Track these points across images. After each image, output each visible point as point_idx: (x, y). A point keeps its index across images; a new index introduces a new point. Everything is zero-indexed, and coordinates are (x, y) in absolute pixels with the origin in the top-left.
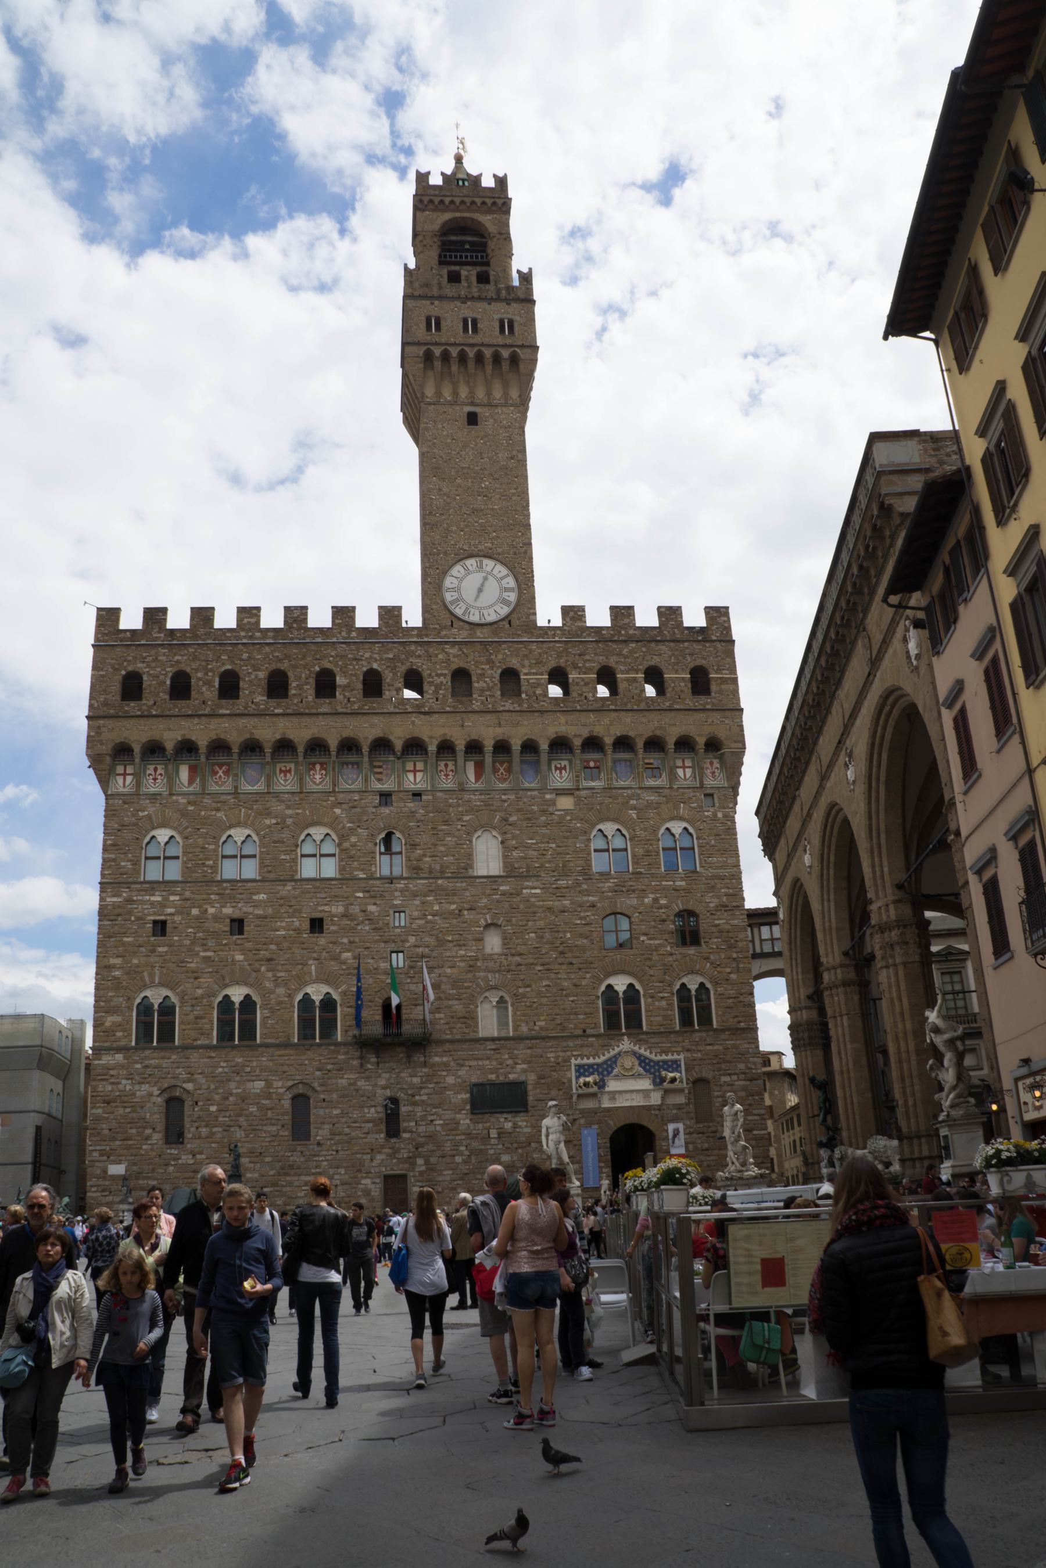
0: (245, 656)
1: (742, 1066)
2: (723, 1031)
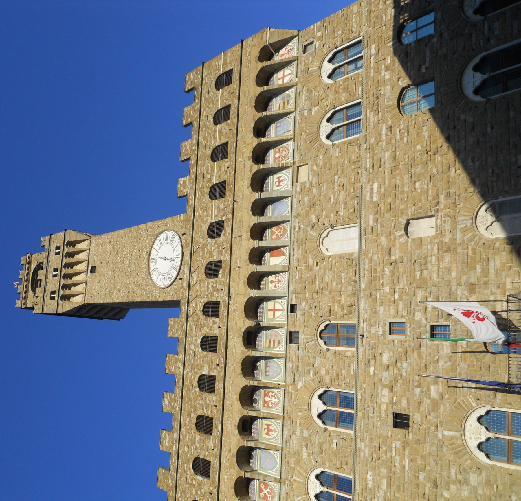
0: (186, 449)
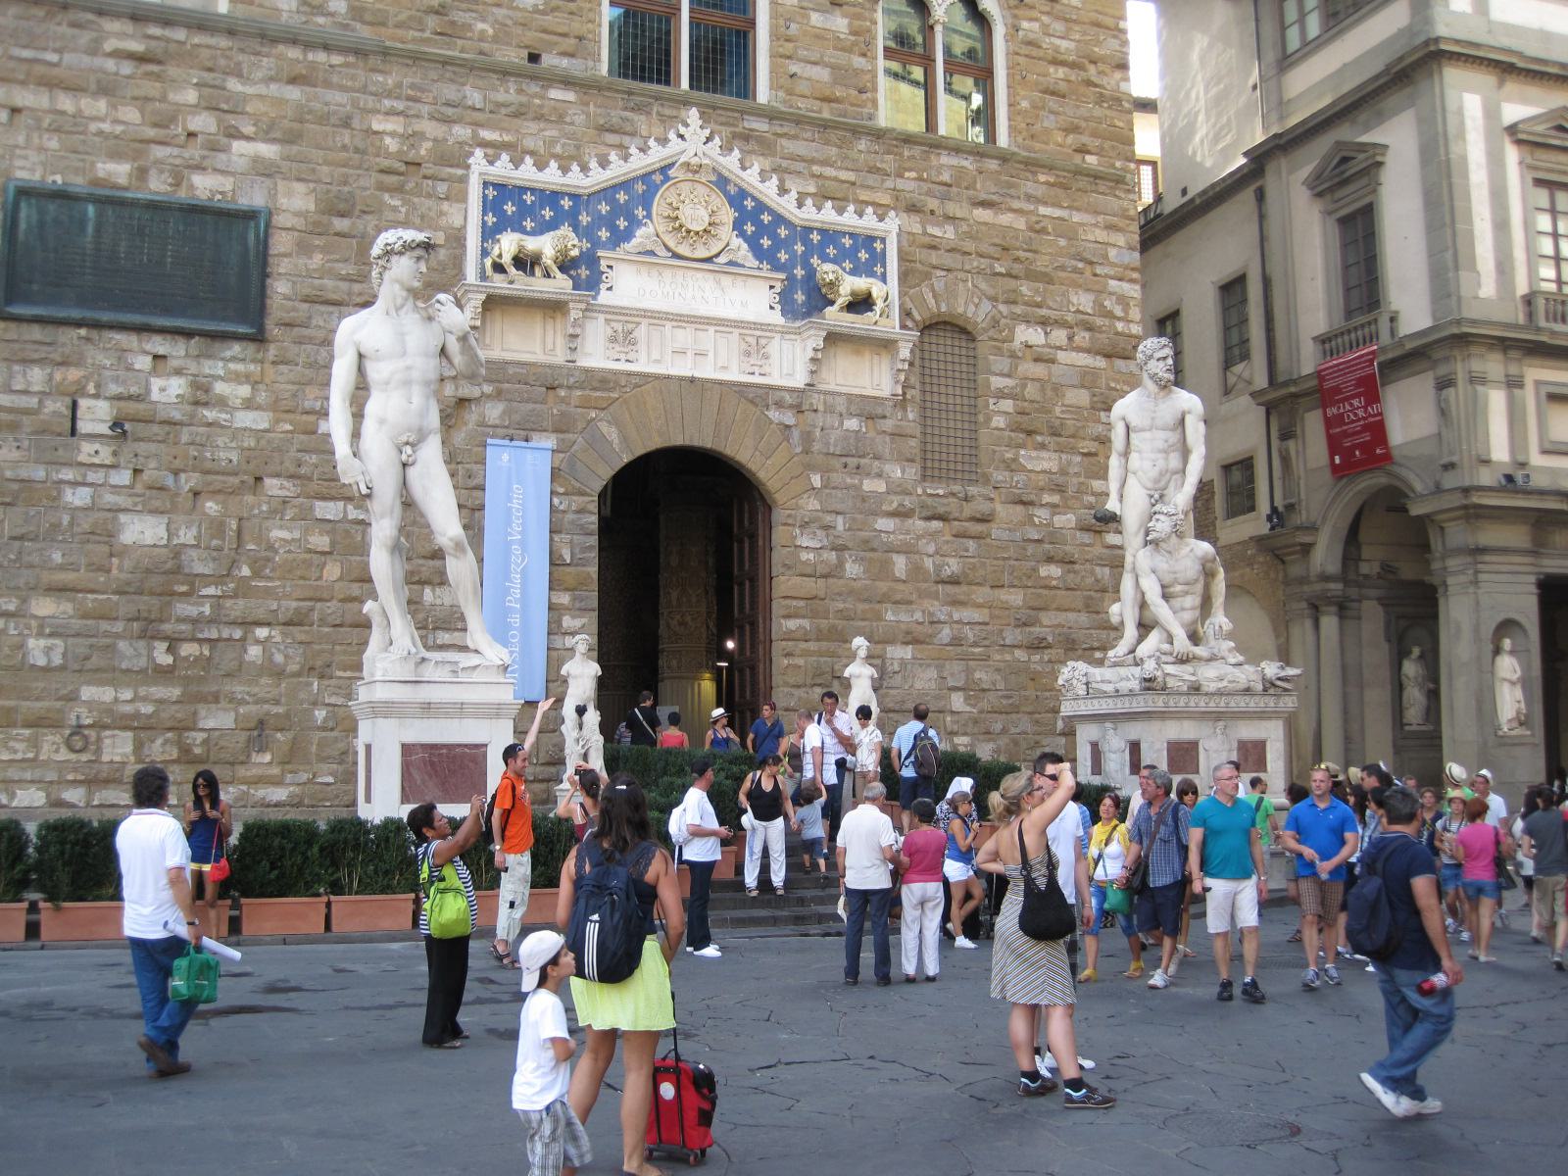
1: (1084, 301)
2: (1032, 165)
